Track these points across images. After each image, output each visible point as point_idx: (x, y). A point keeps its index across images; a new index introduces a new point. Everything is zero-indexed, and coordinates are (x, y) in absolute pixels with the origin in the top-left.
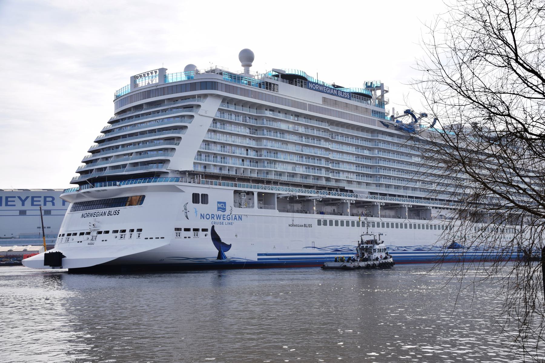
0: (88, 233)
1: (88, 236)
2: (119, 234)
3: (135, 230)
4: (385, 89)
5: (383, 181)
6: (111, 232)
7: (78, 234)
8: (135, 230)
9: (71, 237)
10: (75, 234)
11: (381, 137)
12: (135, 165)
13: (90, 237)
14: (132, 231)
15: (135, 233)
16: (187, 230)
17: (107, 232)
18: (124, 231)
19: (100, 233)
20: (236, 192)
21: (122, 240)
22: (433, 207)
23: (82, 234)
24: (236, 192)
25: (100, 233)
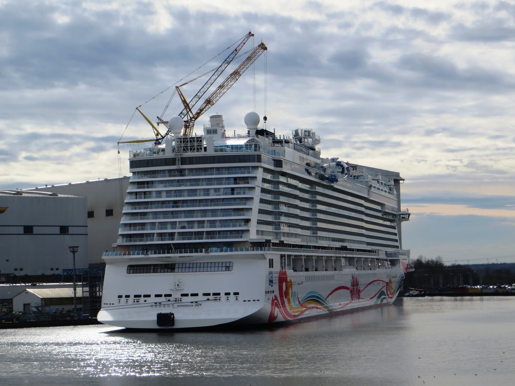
0: (170, 295)
1: (168, 298)
2: (211, 297)
3: (232, 294)
4: (317, 138)
5: (320, 234)
6: (200, 295)
7: (153, 296)
8: (232, 294)
9: (142, 299)
10: (149, 296)
11: (319, 189)
12: (208, 233)
13: (171, 298)
14: (227, 294)
15: (232, 297)
16: (268, 292)
17: (196, 295)
18: (219, 294)
19: (187, 295)
20: (282, 256)
21: (217, 303)
22: (343, 257)
23: (157, 296)
24: (282, 256)
25: (187, 295)
